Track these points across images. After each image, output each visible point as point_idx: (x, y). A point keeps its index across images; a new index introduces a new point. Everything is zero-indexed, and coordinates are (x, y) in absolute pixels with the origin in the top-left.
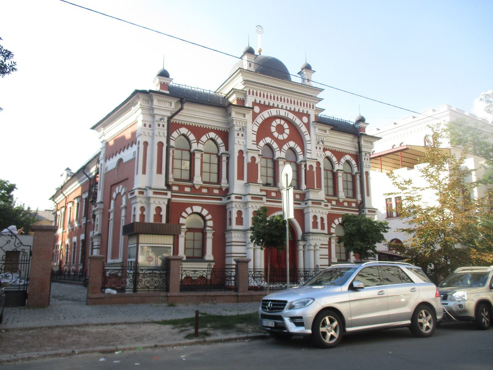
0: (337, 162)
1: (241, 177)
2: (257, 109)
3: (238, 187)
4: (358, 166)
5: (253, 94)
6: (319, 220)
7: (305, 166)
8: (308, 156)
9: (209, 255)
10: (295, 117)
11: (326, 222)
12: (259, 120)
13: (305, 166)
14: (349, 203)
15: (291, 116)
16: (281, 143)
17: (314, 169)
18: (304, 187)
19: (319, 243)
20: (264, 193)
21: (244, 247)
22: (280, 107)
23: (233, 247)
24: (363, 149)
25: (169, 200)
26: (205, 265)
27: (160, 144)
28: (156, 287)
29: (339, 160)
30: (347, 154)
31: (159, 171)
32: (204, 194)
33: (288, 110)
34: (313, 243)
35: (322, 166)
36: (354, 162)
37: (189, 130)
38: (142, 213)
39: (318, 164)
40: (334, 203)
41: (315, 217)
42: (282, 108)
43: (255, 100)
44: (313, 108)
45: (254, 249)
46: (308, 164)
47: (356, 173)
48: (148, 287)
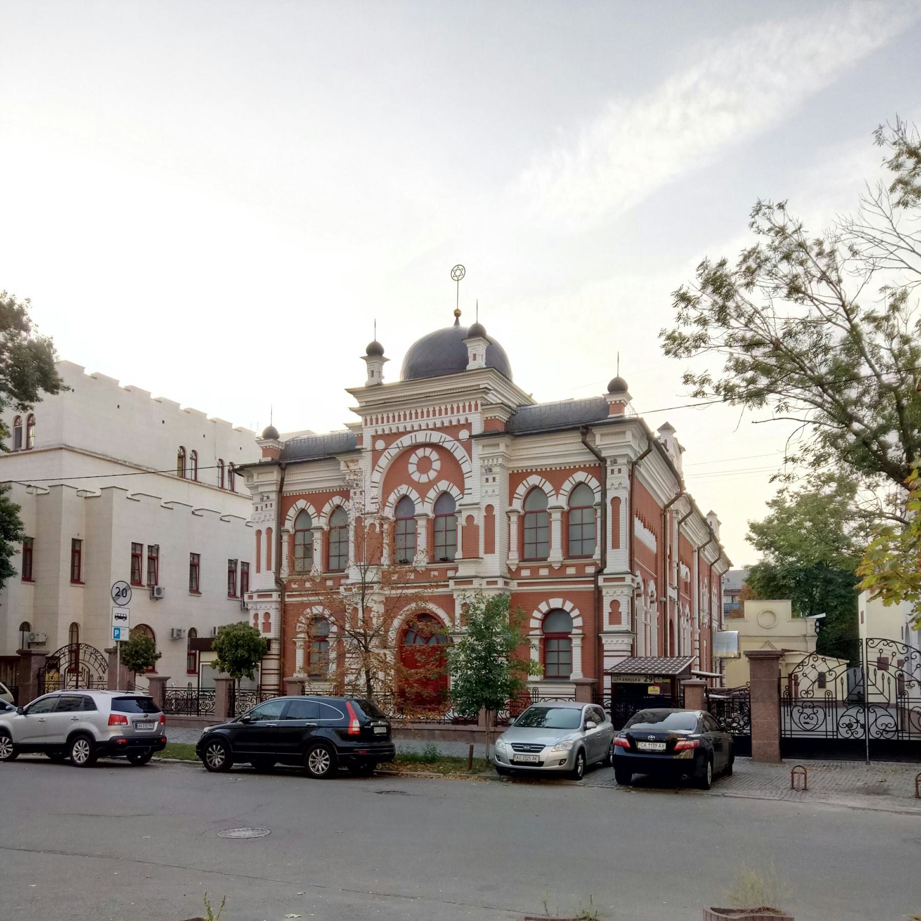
10: (444, 435)
12: (384, 462)
15: (436, 437)
16: (423, 490)
17: (479, 519)
18: (459, 555)
27: (269, 530)
29: (557, 489)
30: (580, 469)
31: (269, 568)
33: (432, 429)
35: (497, 512)
36: (594, 483)
39: (490, 508)
42: (421, 430)
44: (476, 409)
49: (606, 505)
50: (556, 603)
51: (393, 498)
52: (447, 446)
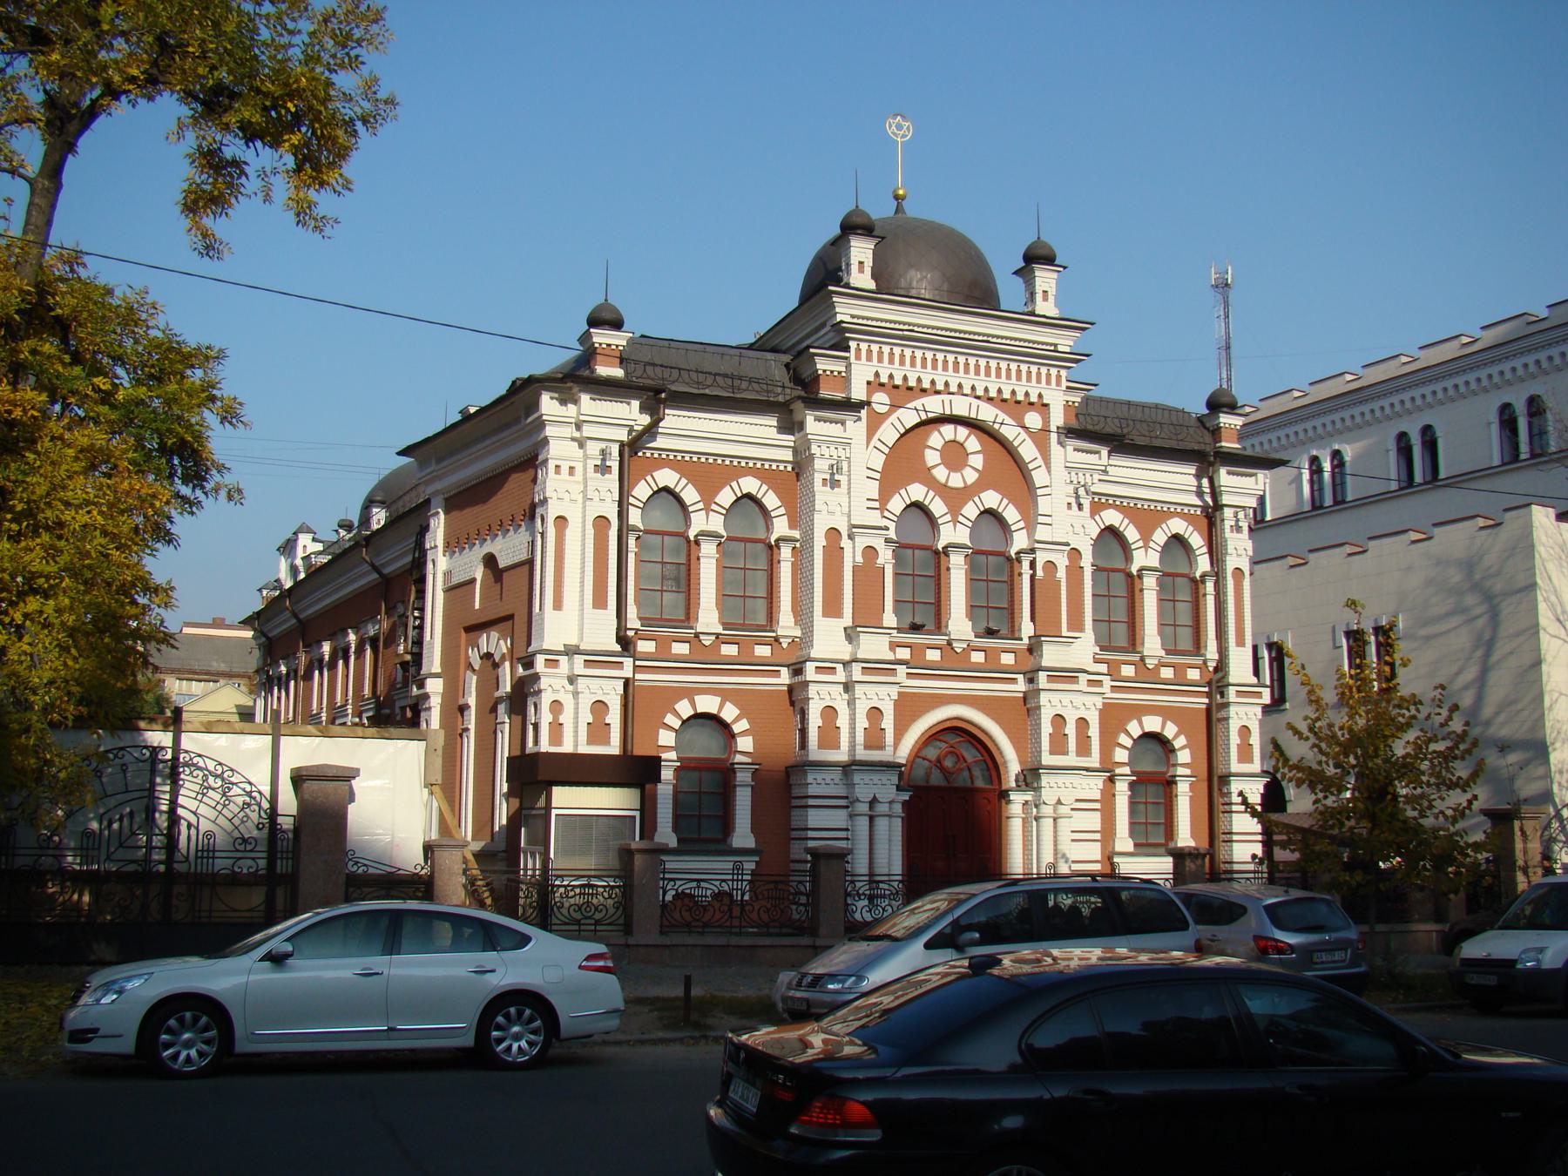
0: (1141, 544)
1: (832, 609)
2: (881, 400)
3: (828, 639)
4: (1210, 552)
5: (869, 358)
6: (1071, 730)
7: (1033, 565)
8: (1042, 533)
9: (743, 836)
11: (1094, 732)
12: (889, 434)
13: (1033, 565)
14: (1179, 670)
15: (987, 413)
17: (1061, 574)
18: (1027, 629)
19: (1068, 797)
20: (904, 654)
21: (843, 813)
22: (953, 388)
23: (811, 812)
24: (1225, 499)
25: (627, 682)
26: (724, 864)
28: (597, 922)
29: (1146, 537)
31: (600, 602)
32: (729, 661)
33: (978, 398)
34: (1048, 795)
36: (1197, 541)
37: (683, 475)
38: (556, 718)
39: (1075, 553)
40: (1128, 671)
41: (1059, 720)
43: (877, 375)
44: (1058, 383)
45: (872, 818)
46: (1041, 558)
47: (1203, 576)
48: (578, 922)
49: (1225, 578)
50: (1152, 724)
51: (897, 505)
52: (1010, 432)
